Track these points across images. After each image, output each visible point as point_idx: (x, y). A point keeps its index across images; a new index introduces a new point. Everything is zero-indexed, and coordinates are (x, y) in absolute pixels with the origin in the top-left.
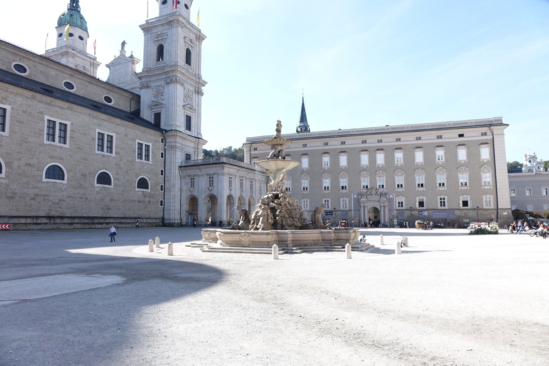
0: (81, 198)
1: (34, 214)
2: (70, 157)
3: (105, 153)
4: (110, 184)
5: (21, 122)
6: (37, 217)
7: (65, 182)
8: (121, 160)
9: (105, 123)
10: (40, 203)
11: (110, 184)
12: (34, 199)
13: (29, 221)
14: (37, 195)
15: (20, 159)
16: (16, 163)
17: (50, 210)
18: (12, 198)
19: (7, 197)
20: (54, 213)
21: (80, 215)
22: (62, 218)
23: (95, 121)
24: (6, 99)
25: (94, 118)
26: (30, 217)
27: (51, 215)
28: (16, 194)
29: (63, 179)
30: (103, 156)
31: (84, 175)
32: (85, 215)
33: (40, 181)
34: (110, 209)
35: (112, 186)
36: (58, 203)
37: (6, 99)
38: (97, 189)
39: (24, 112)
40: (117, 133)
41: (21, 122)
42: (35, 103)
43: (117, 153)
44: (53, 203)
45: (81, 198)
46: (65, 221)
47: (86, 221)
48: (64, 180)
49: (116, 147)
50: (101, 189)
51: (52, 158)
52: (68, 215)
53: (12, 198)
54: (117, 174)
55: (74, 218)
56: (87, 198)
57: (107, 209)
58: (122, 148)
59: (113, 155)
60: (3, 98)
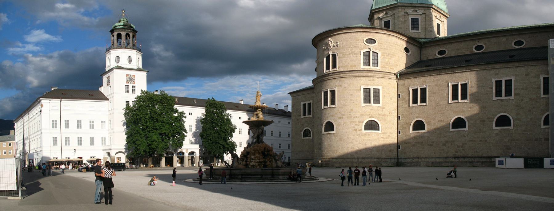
0: (481, 141)
1: (445, 155)
2: (471, 108)
3: (504, 97)
4: (510, 125)
5: (434, 93)
6: (446, 158)
7: (467, 129)
8: (522, 100)
9: (502, 71)
10: (449, 147)
11: (510, 125)
12: (444, 145)
13: (441, 160)
14: (447, 142)
15: (435, 118)
16: (433, 122)
17: (456, 152)
18: (431, 145)
19: (428, 145)
20: (459, 154)
21: (480, 155)
22: (464, 157)
23: (492, 72)
24: (425, 82)
25: (491, 69)
26: (442, 158)
27: (457, 156)
28: (433, 142)
29: (465, 127)
30: (502, 100)
31: (483, 121)
32: (484, 155)
33: (448, 131)
34: (510, 149)
35: (512, 127)
36: (462, 146)
37: (425, 82)
38: (497, 132)
39: (436, 85)
40: (516, 76)
41: (434, 93)
42: (443, 76)
43: (515, 94)
44: (458, 147)
45: (481, 141)
46: (467, 160)
47: (484, 160)
48: (465, 127)
49: (516, 89)
50: (500, 131)
51: (456, 112)
52: (470, 155)
53: (431, 145)
54: (518, 114)
55: (474, 158)
56: (486, 141)
57: (507, 149)
58: (522, 89)
59: (513, 97)
60: (423, 81)
